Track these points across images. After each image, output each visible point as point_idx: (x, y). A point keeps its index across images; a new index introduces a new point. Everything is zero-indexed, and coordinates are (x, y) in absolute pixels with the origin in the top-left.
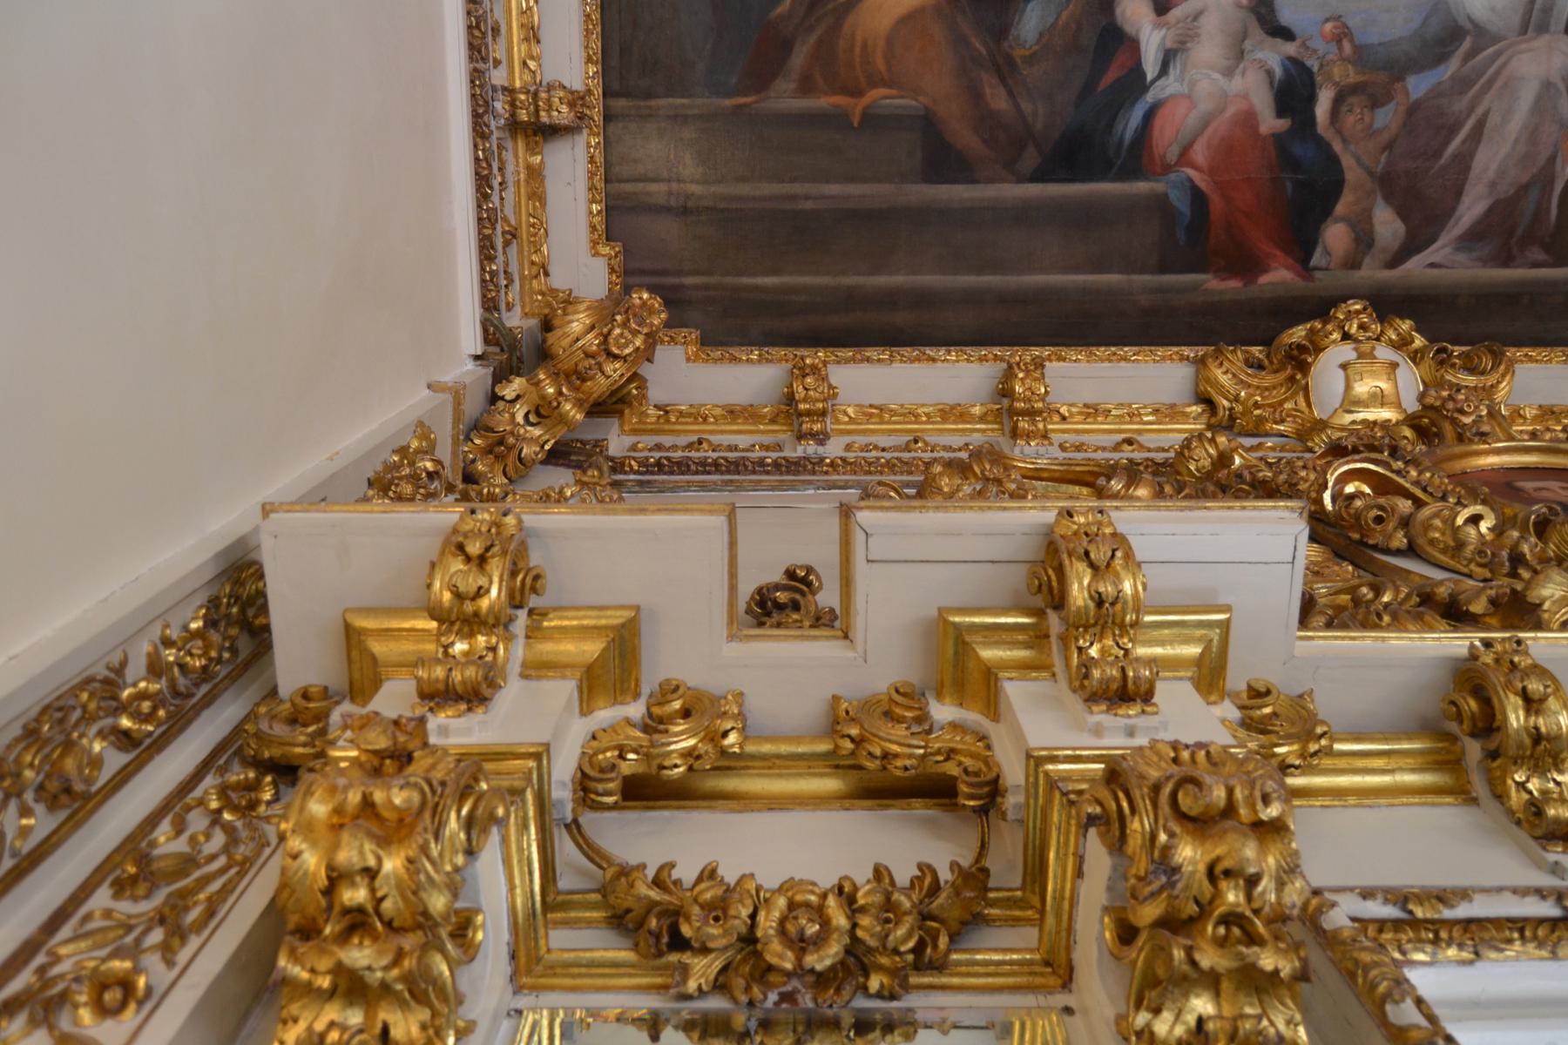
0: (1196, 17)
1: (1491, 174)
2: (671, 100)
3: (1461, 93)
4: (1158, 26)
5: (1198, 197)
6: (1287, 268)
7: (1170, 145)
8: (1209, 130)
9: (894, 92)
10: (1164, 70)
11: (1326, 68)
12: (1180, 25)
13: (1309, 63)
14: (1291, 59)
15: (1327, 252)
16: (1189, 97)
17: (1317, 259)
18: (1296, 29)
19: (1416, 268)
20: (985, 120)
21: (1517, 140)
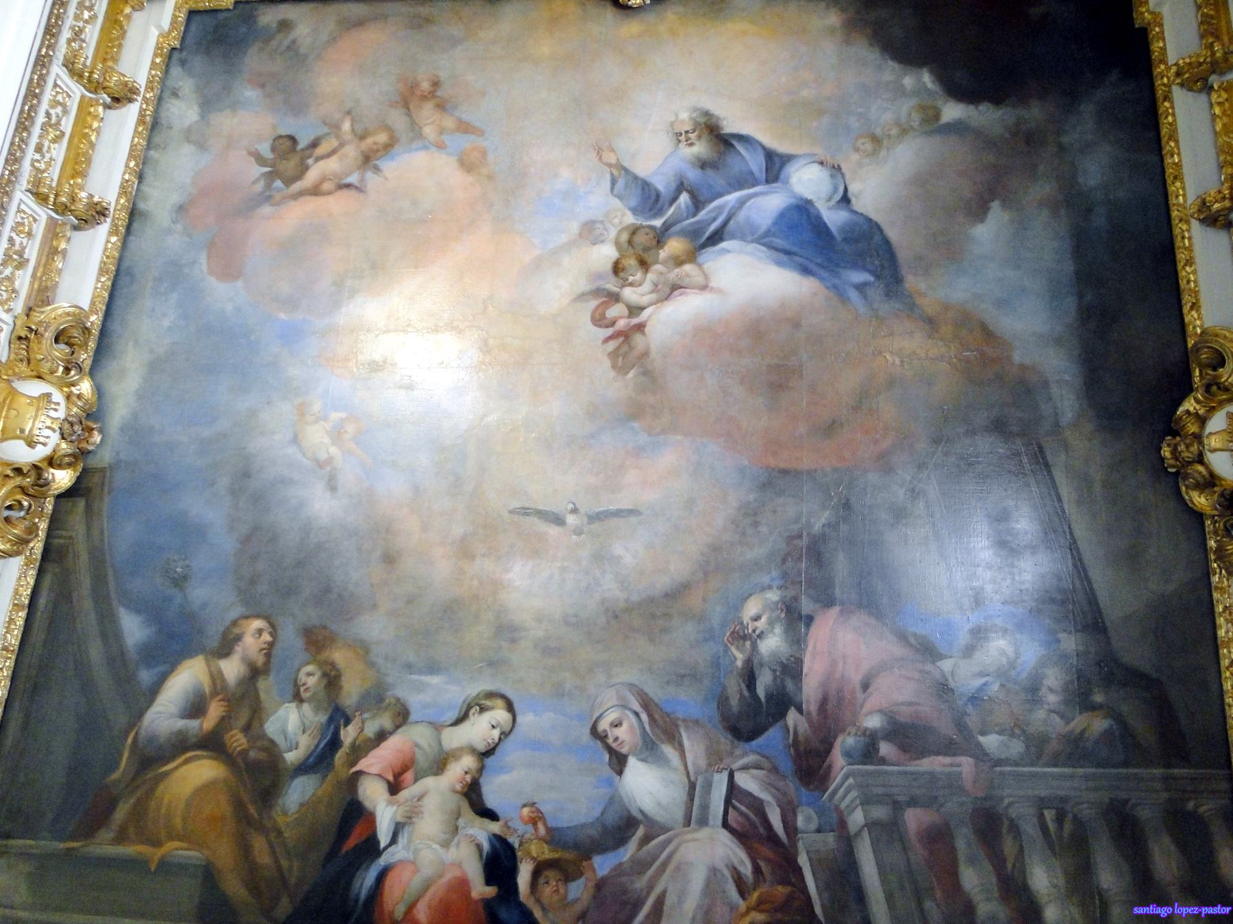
3: (639, 873)
4: (390, 803)
7: (398, 904)
9: (184, 845)
10: (394, 841)
13: (511, 840)
14: (495, 835)
16: (413, 863)
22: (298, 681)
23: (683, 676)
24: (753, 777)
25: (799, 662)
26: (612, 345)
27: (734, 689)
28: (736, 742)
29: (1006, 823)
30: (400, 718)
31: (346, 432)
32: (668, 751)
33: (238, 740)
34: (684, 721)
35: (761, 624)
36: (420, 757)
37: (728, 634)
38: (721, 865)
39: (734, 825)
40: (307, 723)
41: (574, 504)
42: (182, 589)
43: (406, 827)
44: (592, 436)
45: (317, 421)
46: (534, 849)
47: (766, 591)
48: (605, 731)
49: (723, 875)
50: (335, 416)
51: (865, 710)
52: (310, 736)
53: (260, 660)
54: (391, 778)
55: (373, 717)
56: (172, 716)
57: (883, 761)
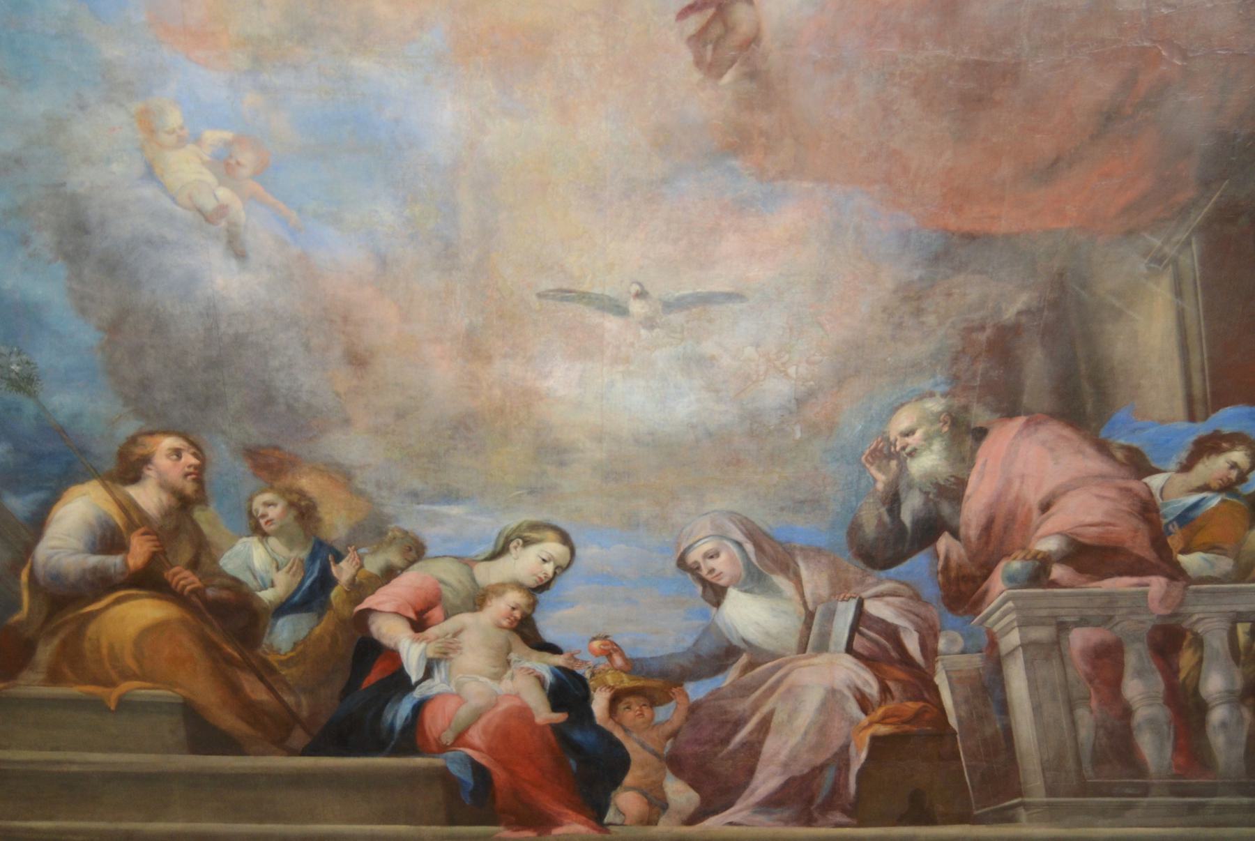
0: (456, 635)
1: (783, 756)
4: (418, 640)
5: (478, 769)
6: (583, 824)
7: (444, 731)
9: (148, 684)
10: (428, 674)
13: (580, 671)
14: (559, 668)
15: (620, 812)
16: (458, 695)
17: (610, 816)
20: (250, 710)
21: (806, 733)
22: (255, 514)
23: (802, 502)
24: (888, 604)
25: (962, 483)
26: (694, 23)
27: (872, 518)
28: (869, 570)
29: (1189, 636)
30: (413, 554)
31: (238, 163)
32: (780, 581)
33: (184, 578)
34: (802, 549)
35: (913, 441)
36: (447, 592)
37: (867, 452)
38: (839, 685)
39: (861, 650)
40: (280, 559)
41: (640, 284)
42: (32, 395)
43: (442, 664)
44: (664, 181)
45: (181, 142)
46: (610, 679)
47: (925, 400)
48: (696, 562)
49: (844, 695)
50: (213, 136)
51: (1040, 532)
52: (288, 572)
53: (189, 487)
54: (412, 615)
55: (374, 553)
56: (77, 552)
57: (1054, 584)
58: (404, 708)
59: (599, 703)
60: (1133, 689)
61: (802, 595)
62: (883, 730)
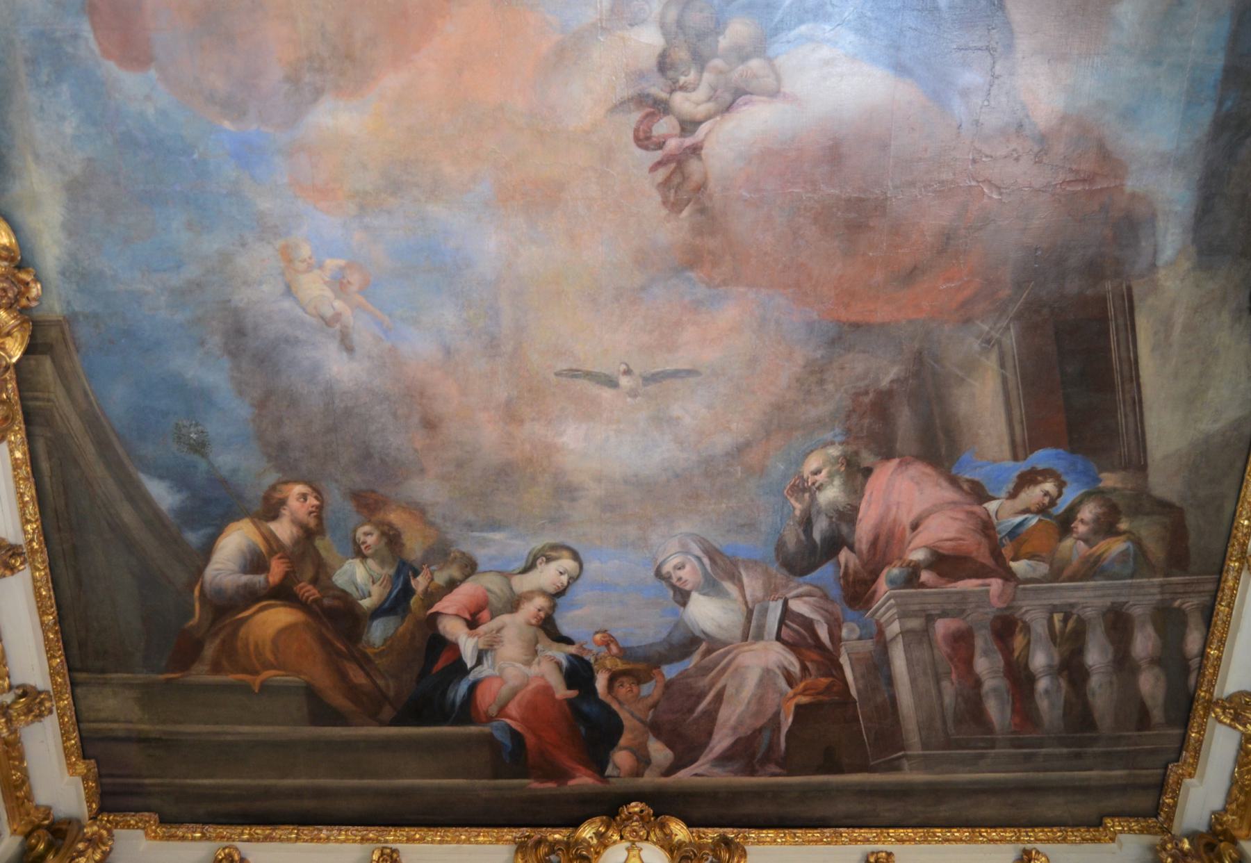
0: (499, 630)
1: (732, 722)
2: (119, 675)
3: (703, 675)
4: (470, 636)
5: (515, 735)
6: (589, 776)
7: (490, 705)
8: (518, 697)
10: (479, 661)
11: (600, 661)
12: (487, 636)
13: (587, 658)
14: (572, 655)
15: (616, 767)
16: (500, 677)
17: (609, 771)
18: (573, 637)
19: (684, 776)
20: (352, 691)
21: (749, 703)
22: (358, 541)
23: (743, 526)
24: (805, 602)
25: (855, 509)
26: (661, 174)
27: (792, 538)
28: (791, 576)
29: (1020, 624)
30: (468, 569)
31: (349, 282)
32: (729, 586)
33: (308, 591)
34: (743, 561)
35: (821, 478)
36: (492, 598)
37: (788, 487)
38: (772, 665)
39: (786, 638)
40: (375, 575)
41: (626, 364)
42: (204, 455)
43: (489, 654)
44: (643, 288)
45: (310, 268)
46: (608, 664)
47: (828, 447)
48: (668, 573)
49: (775, 673)
50: (332, 263)
51: (912, 546)
52: (380, 585)
53: (312, 522)
54: (467, 616)
55: (441, 569)
56: (234, 572)
57: (923, 585)
58: (463, 688)
59: (601, 683)
60: (982, 665)
61: (744, 596)
62: (804, 700)
